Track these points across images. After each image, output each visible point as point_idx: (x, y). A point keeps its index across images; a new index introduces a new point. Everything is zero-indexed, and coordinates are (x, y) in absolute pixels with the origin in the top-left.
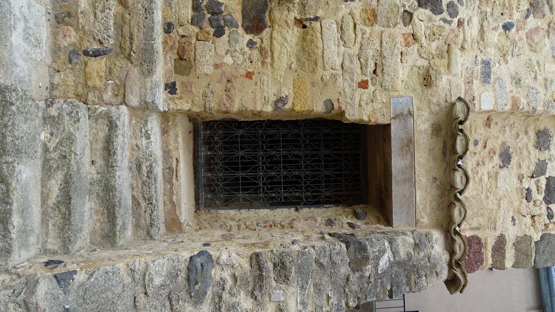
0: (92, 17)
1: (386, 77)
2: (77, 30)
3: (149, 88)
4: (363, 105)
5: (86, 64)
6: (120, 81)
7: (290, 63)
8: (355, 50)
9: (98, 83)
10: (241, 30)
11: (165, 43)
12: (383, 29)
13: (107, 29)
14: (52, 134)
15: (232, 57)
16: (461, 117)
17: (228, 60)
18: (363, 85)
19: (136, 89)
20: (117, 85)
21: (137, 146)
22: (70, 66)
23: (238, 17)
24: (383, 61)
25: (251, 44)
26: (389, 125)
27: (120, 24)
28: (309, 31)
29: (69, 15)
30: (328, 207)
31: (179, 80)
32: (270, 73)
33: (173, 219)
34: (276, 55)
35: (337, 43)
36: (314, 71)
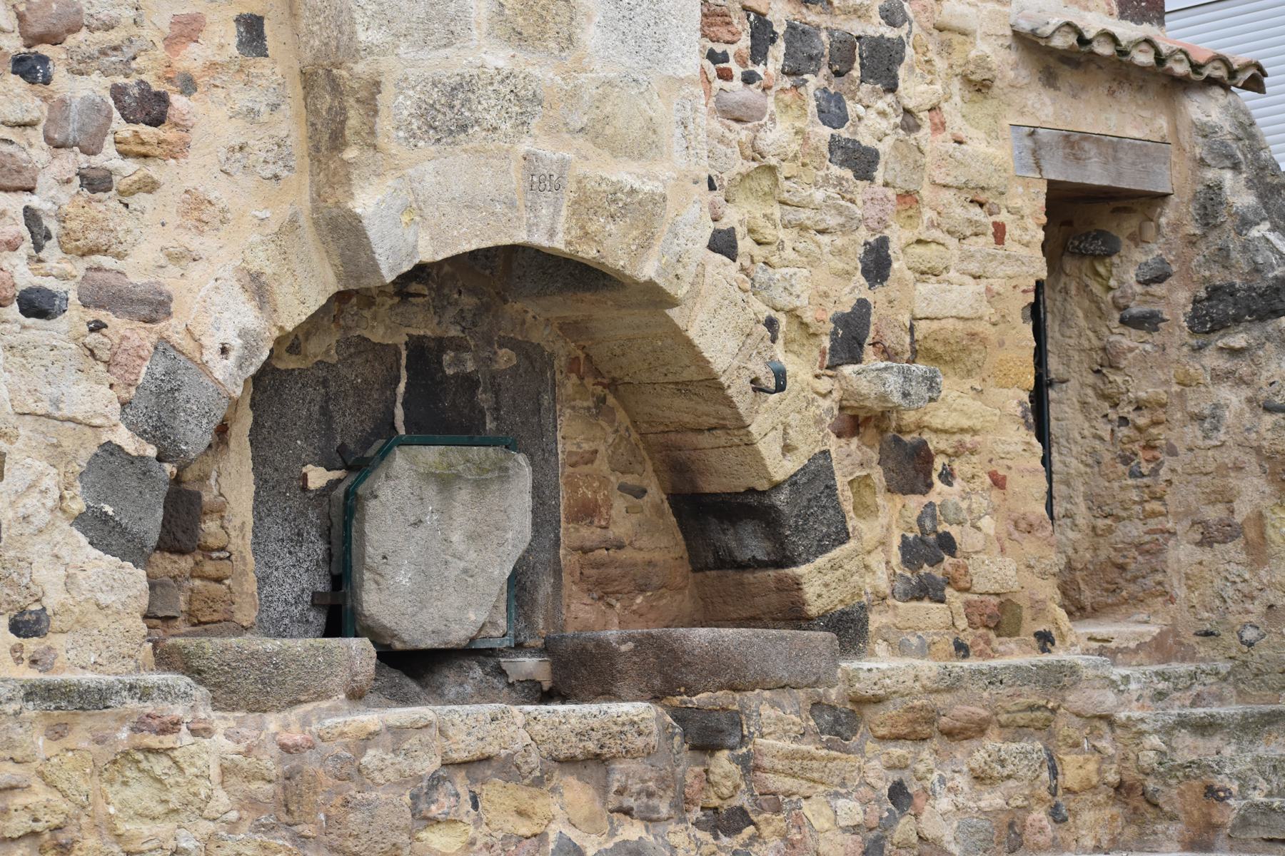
0: (1011, 783)
1: (993, 182)
2: (1026, 809)
3: (1095, 672)
4: (1028, 238)
5: (1069, 790)
6: (1084, 726)
7: (972, 393)
8: (952, 242)
9: (1092, 767)
10: (933, 497)
11: (981, 654)
12: (926, 179)
13: (1025, 754)
14: (1255, 788)
15: (980, 518)
16: (1072, 39)
17: (987, 523)
18: (999, 232)
19: (1096, 695)
20: (1091, 733)
21: (1138, 700)
22: (1070, 820)
23: (915, 503)
24: (972, 185)
25: (947, 477)
26: (1051, 183)
27: (1016, 730)
28: (927, 346)
29: (1011, 825)
30: (1045, 308)
31: (1031, 626)
32: (990, 437)
33: (1157, 649)
34: (965, 423)
35: (944, 286)
36: (984, 341)
